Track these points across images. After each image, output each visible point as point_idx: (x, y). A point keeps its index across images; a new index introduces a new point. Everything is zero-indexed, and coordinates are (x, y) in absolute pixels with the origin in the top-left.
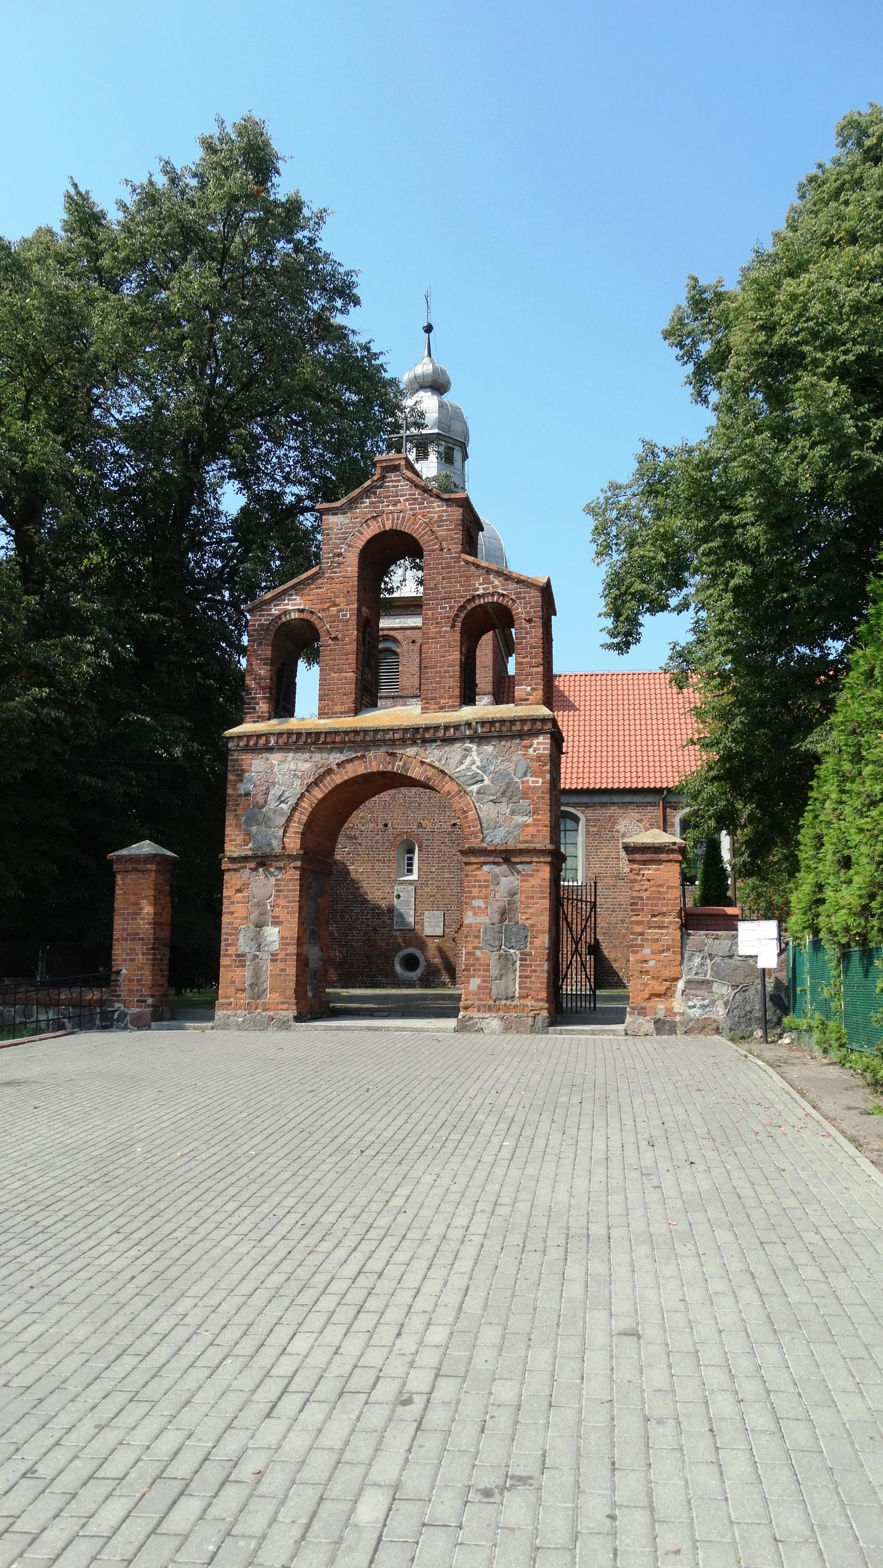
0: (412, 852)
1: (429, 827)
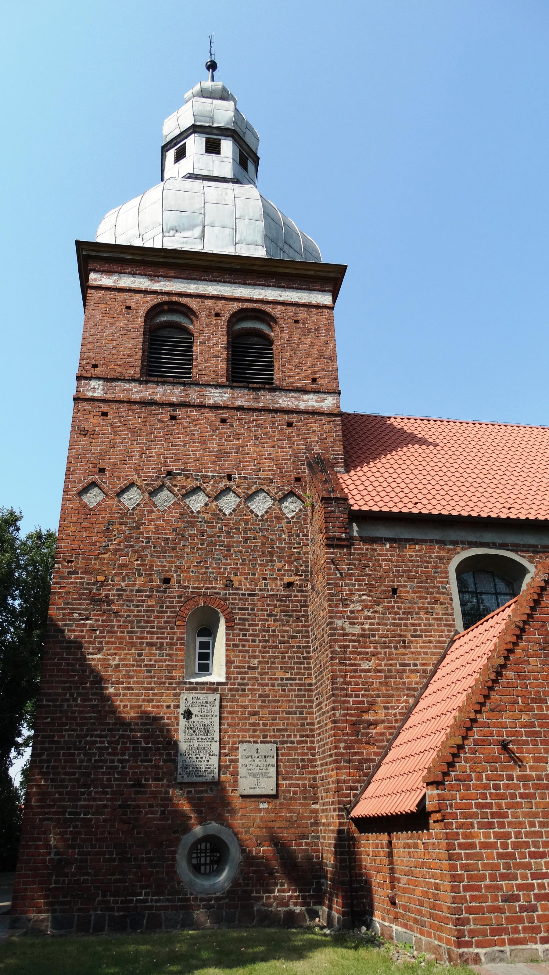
0: (208, 631)
1: (246, 586)
